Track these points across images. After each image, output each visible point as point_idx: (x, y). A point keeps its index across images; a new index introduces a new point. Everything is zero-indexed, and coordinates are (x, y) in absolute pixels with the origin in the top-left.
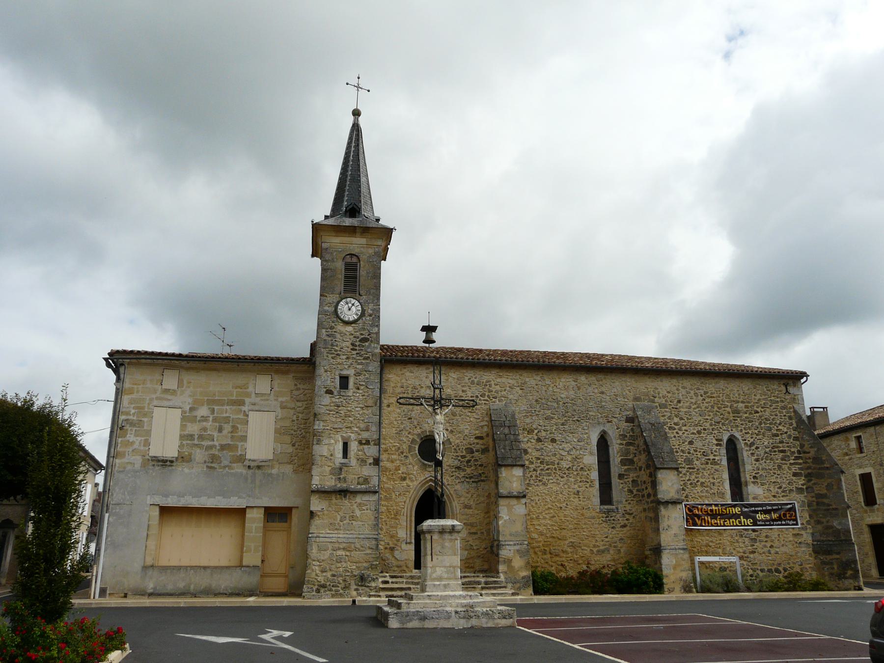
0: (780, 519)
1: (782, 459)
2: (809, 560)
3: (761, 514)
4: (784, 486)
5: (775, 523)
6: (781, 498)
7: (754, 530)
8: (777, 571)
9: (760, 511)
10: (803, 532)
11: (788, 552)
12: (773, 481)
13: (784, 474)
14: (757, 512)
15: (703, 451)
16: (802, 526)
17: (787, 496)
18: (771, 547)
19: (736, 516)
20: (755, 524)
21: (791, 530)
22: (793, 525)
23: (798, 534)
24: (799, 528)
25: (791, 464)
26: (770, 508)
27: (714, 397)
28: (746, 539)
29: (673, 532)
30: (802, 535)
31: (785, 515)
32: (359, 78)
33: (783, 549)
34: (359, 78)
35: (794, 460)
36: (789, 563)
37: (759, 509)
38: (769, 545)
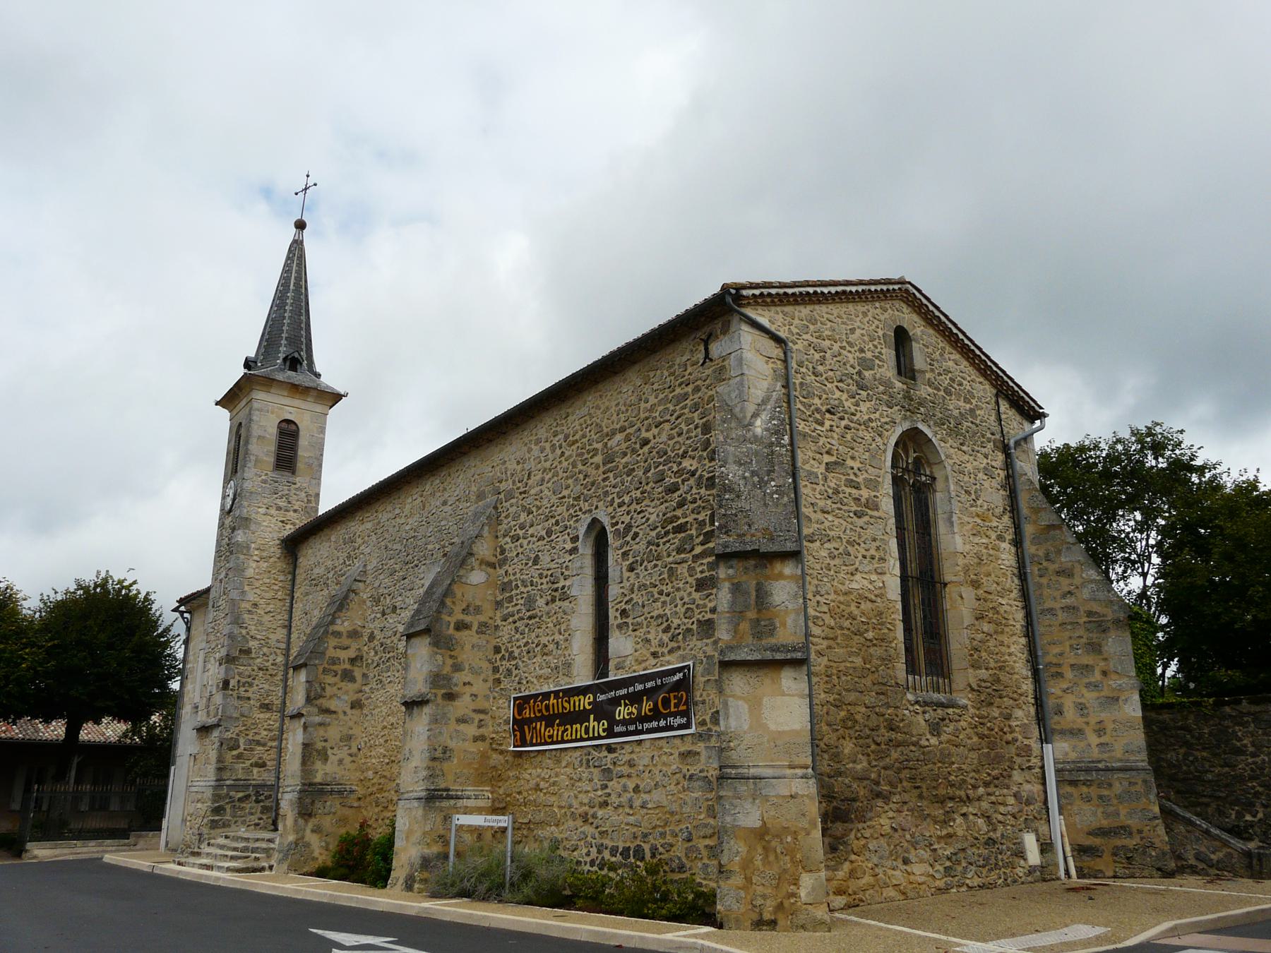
0: (656, 715)
1: (680, 550)
2: (706, 826)
3: (626, 705)
4: (676, 622)
5: (646, 726)
6: (668, 658)
7: (610, 749)
8: (639, 853)
9: (624, 697)
10: (700, 747)
11: (665, 803)
12: (655, 614)
13: (678, 590)
14: (616, 702)
15: (549, 573)
16: (700, 729)
17: (679, 648)
18: (636, 789)
19: (581, 717)
20: (611, 733)
21: (678, 742)
22: (681, 727)
23: (689, 752)
24: (692, 735)
25: (696, 558)
26: (639, 687)
27: (576, 441)
28: (596, 771)
29: (414, 764)
30: (698, 753)
31: (666, 702)
32: (308, 176)
33: (657, 796)
34: (308, 176)
35: (702, 544)
36: (663, 835)
37: (623, 692)
38: (631, 785)
